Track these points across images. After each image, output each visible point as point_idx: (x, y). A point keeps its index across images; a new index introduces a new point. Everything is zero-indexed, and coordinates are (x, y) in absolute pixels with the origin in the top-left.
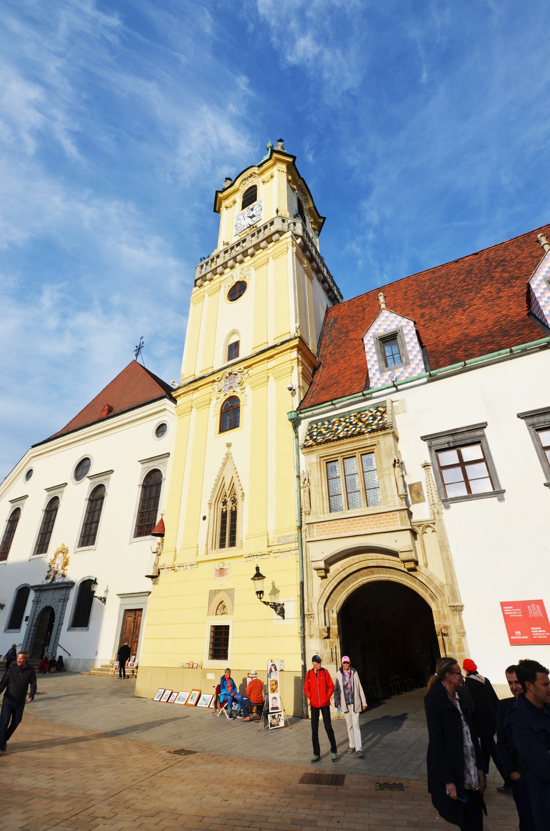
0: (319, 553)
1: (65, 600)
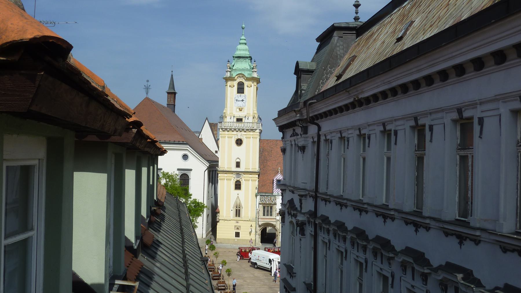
0: (260, 223)
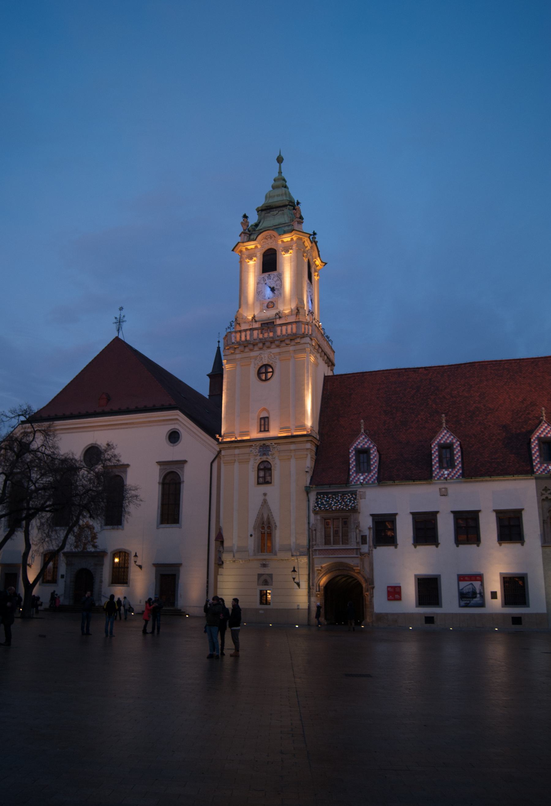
1: (102, 565)
